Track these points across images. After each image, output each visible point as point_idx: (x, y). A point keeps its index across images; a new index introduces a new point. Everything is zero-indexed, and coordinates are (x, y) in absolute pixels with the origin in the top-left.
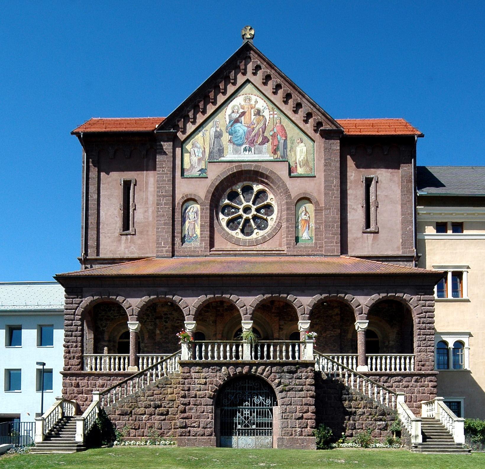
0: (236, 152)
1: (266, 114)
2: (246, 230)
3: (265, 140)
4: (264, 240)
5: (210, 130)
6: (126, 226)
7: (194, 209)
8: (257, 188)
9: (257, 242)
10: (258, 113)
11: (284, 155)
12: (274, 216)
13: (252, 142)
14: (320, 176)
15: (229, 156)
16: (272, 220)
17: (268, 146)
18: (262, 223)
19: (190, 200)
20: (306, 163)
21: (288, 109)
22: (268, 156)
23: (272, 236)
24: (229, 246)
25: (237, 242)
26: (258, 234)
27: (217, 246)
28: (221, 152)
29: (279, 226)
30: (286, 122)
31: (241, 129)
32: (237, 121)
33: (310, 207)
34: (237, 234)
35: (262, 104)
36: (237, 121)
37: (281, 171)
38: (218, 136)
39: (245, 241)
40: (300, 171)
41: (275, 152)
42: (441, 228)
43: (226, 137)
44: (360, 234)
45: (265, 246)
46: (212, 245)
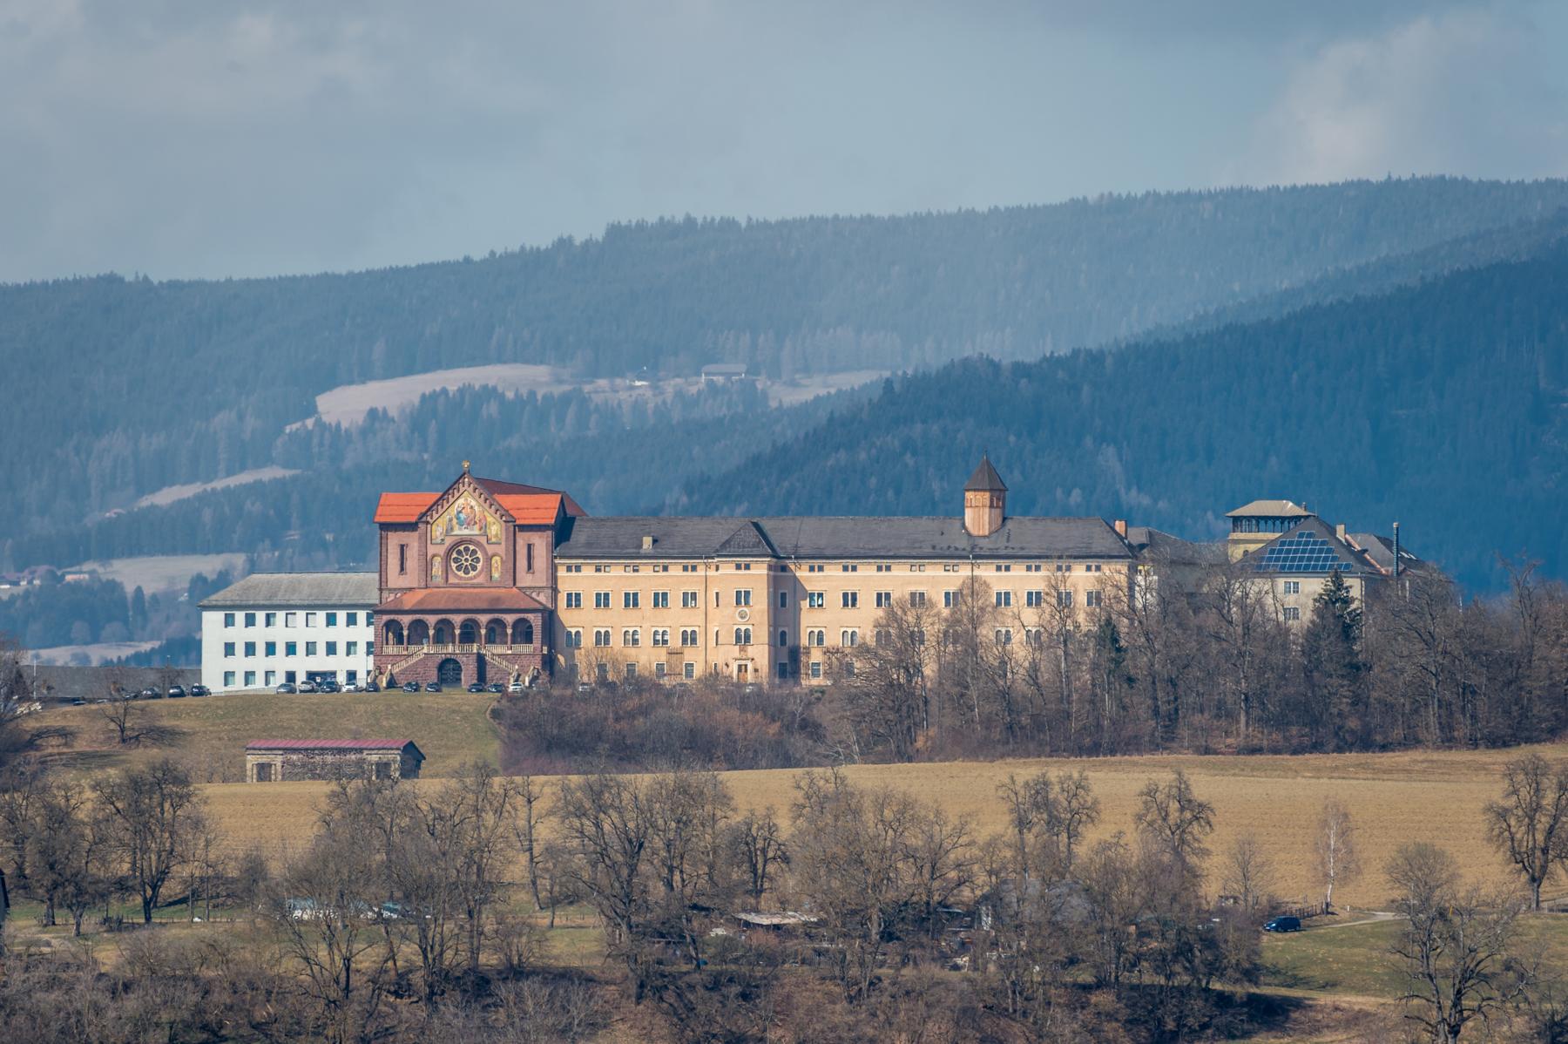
0: (460, 529)
1: (476, 508)
2: (466, 572)
3: (475, 523)
4: (475, 577)
5: (446, 517)
6: (402, 569)
7: (437, 560)
8: (472, 547)
9: (471, 579)
10: (472, 507)
11: (485, 532)
12: (481, 564)
13: (469, 524)
14: (503, 543)
15: (456, 532)
16: (479, 566)
17: (477, 527)
18: (474, 568)
19: (434, 556)
20: (496, 536)
21: (486, 506)
22: (477, 532)
23: (478, 575)
24: (456, 581)
25: (461, 578)
26: (472, 574)
27: (450, 581)
28: (452, 529)
29: (482, 570)
30: (486, 513)
31: (462, 516)
32: (460, 512)
33: (498, 558)
34: (461, 574)
35: (473, 503)
36: (460, 512)
37: (483, 540)
38: (451, 520)
39: (465, 579)
40: (494, 540)
41: (480, 529)
42: (569, 569)
43: (455, 521)
44: (524, 574)
45: (475, 581)
46: (447, 580)
